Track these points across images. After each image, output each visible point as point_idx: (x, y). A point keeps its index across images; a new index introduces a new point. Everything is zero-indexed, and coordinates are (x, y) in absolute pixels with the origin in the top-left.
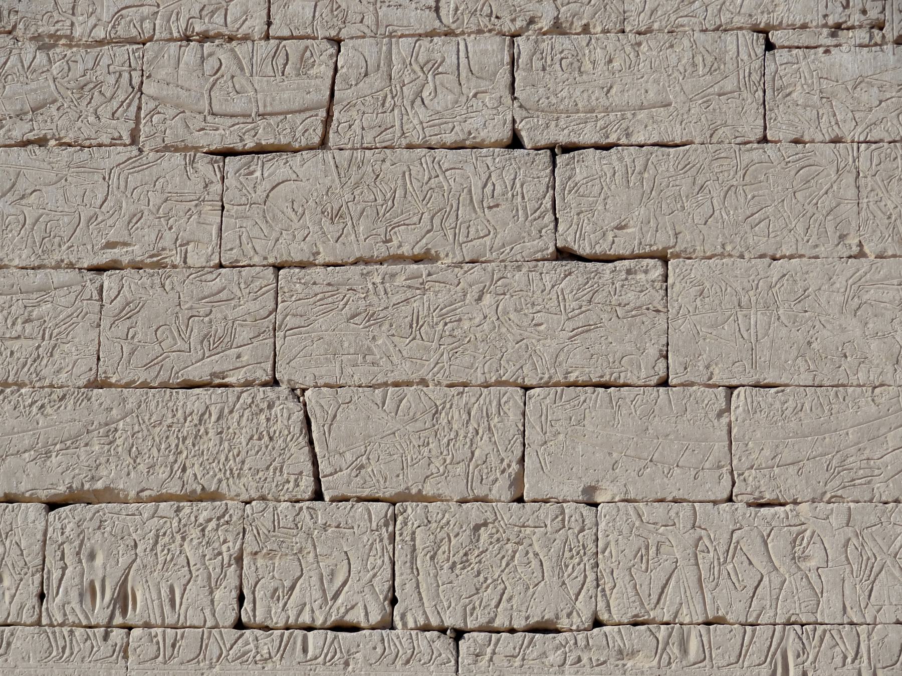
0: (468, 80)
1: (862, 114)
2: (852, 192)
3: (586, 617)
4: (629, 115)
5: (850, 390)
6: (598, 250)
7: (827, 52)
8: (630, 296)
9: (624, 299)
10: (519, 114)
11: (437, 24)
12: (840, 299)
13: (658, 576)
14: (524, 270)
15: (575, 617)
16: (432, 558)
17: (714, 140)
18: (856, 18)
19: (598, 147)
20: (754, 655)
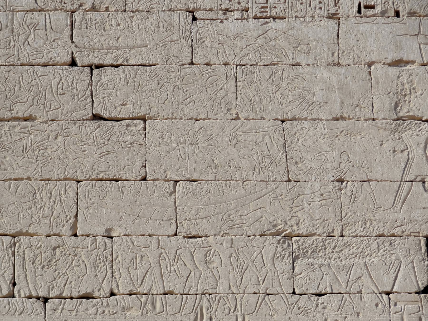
0: (51, 33)
1: (238, 52)
2: (233, 88)
3: (107, 292)
4: (128, 51)
5: (232, 183)
6: (113, 115)
7: (222, 22)
8: (128, 137)
9: (125, 139)
10: (75, 50)
11: (35, 6)
12: (227, 139)
13: (142, 272)
14: (77, 125)
15: (102, 292)
16: (33, 263)
17: (168, 63)
18: (235, 6)
19: (113, 66)
20: (187, 309)
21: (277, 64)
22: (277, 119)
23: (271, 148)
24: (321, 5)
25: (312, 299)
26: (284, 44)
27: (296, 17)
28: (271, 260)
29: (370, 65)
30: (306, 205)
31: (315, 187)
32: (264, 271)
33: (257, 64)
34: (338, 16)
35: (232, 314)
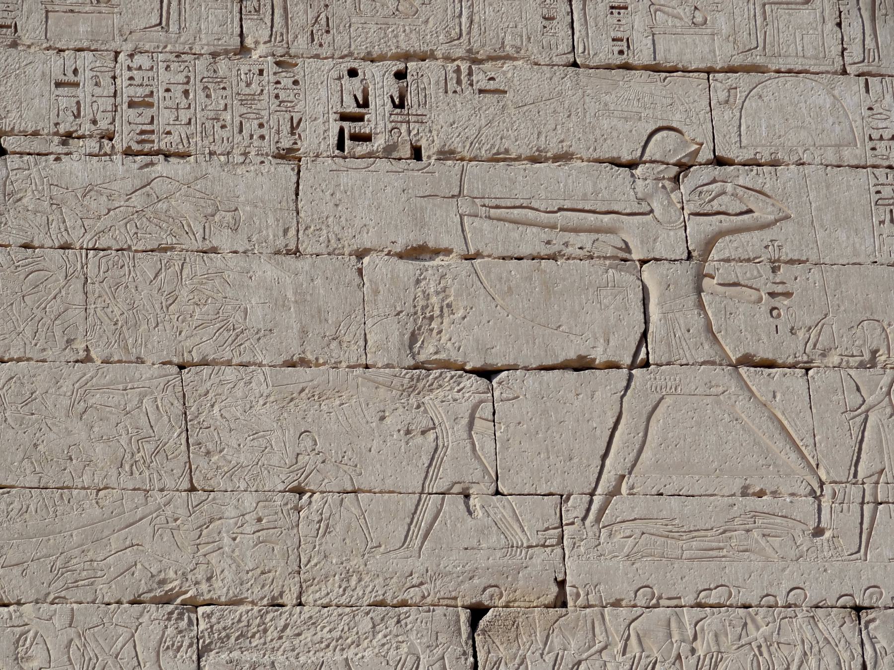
2: (81, 296)
5: (75, 492)
7: (57, 159)
12: (66, 402)
18: (86, 128)
21: (172, 249)
22: (170, 363)
23: (157, 421)
24: (264, 131)
26: (186, 208)
27: (211, 154)
28: (154, 654)
29: (360, 255)
30: (226, 540)
31: (246, 504)
33: (129, 248)
34: (298, 154)
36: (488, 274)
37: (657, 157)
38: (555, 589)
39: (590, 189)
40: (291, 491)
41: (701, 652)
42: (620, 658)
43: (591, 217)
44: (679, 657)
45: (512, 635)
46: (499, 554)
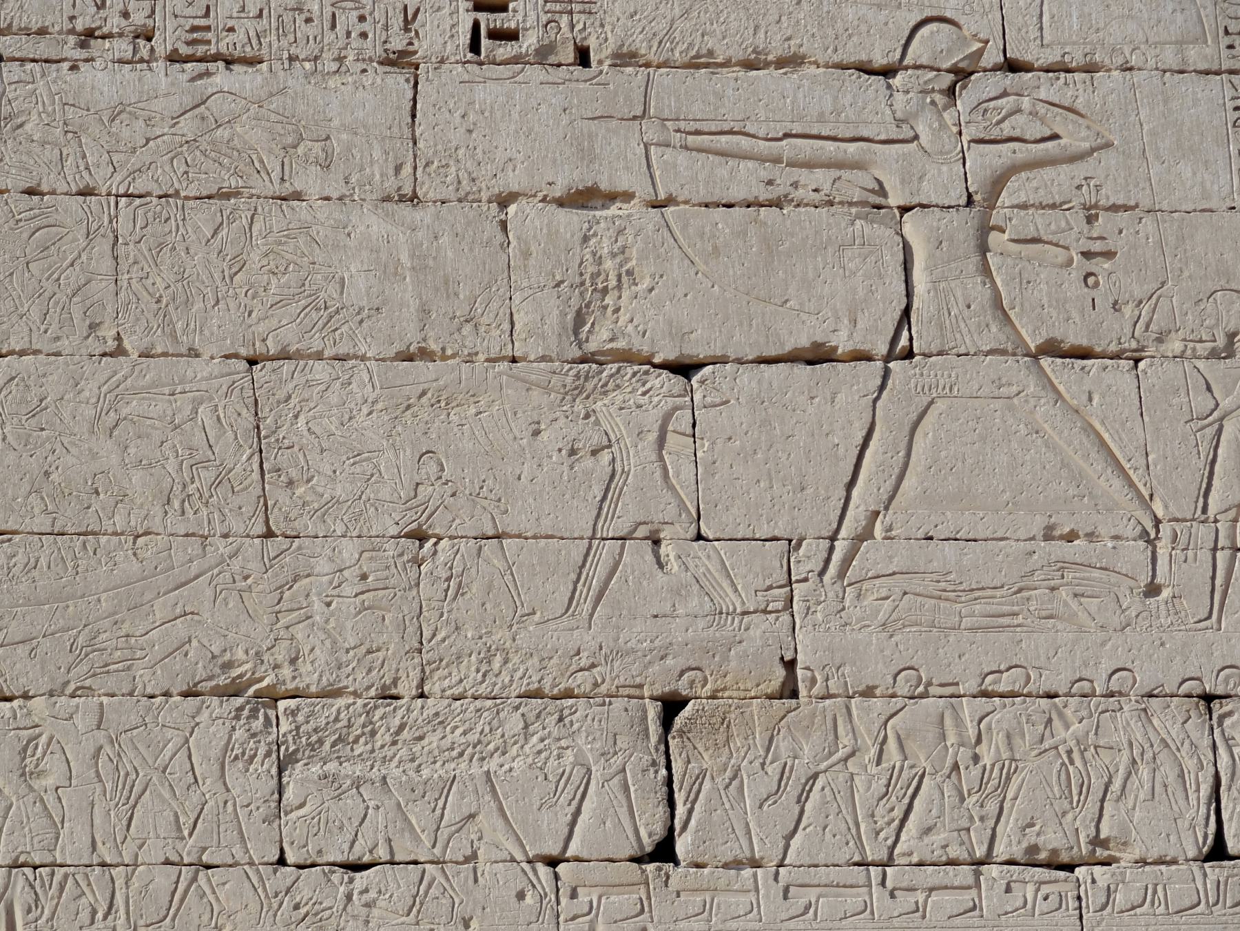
1: (121, 156)
2: (108, 263)
5: (103, 539)
7: (74, 68)
12: (90, 412)
18: (114, 23)
21: (237, 194)
22: (236, 356)
23: (218, 438)
24: (366, 27)
25: (335, 878)
27: (292, 59)
28: (216, 767)
29: (504, 202)
30: (317, 606)
31: (345, 555)
32: (195, 798)
33: (177, 193)
34: (414, 59)
35: (99, 924)
36: (685, 228)
37: (924, 61)
38: (780, 673)
39: (828, 105)
40: (407, 536)
41: (987, 760)
42: (873, 770)
43: (830, 146)
44: (956, 767)
45: (721, 738)
46: (701, 623)
